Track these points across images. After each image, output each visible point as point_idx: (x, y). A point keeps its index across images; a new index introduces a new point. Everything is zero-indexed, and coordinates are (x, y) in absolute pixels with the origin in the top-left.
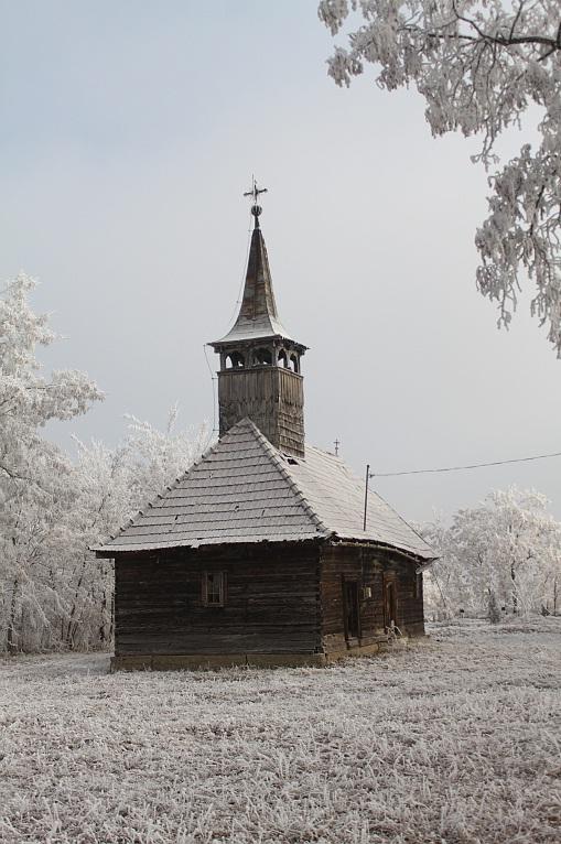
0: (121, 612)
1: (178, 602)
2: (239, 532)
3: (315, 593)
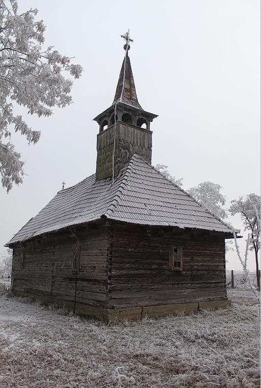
1: (154, 267)
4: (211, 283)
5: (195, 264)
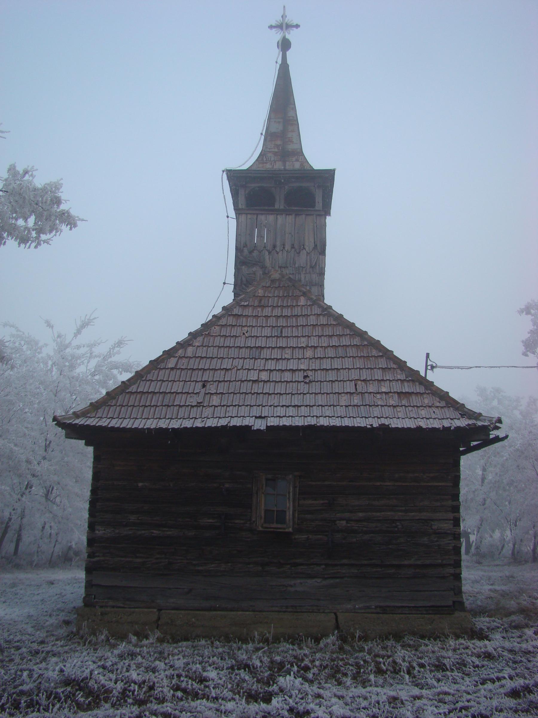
0: (100, 532)
2: (328, 411)
3: (451, 515)
4: (399, 566)
5: (338, 515)
